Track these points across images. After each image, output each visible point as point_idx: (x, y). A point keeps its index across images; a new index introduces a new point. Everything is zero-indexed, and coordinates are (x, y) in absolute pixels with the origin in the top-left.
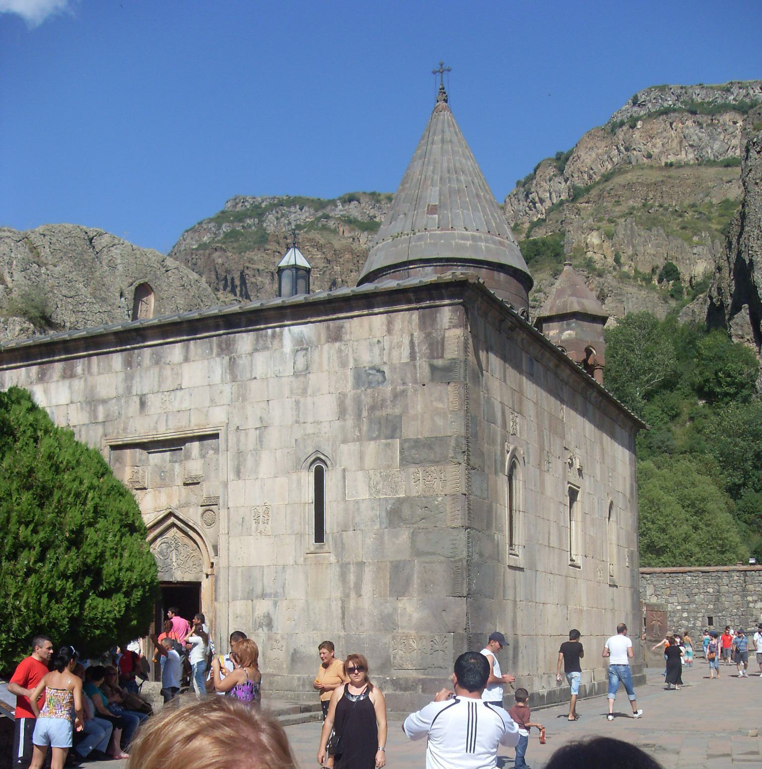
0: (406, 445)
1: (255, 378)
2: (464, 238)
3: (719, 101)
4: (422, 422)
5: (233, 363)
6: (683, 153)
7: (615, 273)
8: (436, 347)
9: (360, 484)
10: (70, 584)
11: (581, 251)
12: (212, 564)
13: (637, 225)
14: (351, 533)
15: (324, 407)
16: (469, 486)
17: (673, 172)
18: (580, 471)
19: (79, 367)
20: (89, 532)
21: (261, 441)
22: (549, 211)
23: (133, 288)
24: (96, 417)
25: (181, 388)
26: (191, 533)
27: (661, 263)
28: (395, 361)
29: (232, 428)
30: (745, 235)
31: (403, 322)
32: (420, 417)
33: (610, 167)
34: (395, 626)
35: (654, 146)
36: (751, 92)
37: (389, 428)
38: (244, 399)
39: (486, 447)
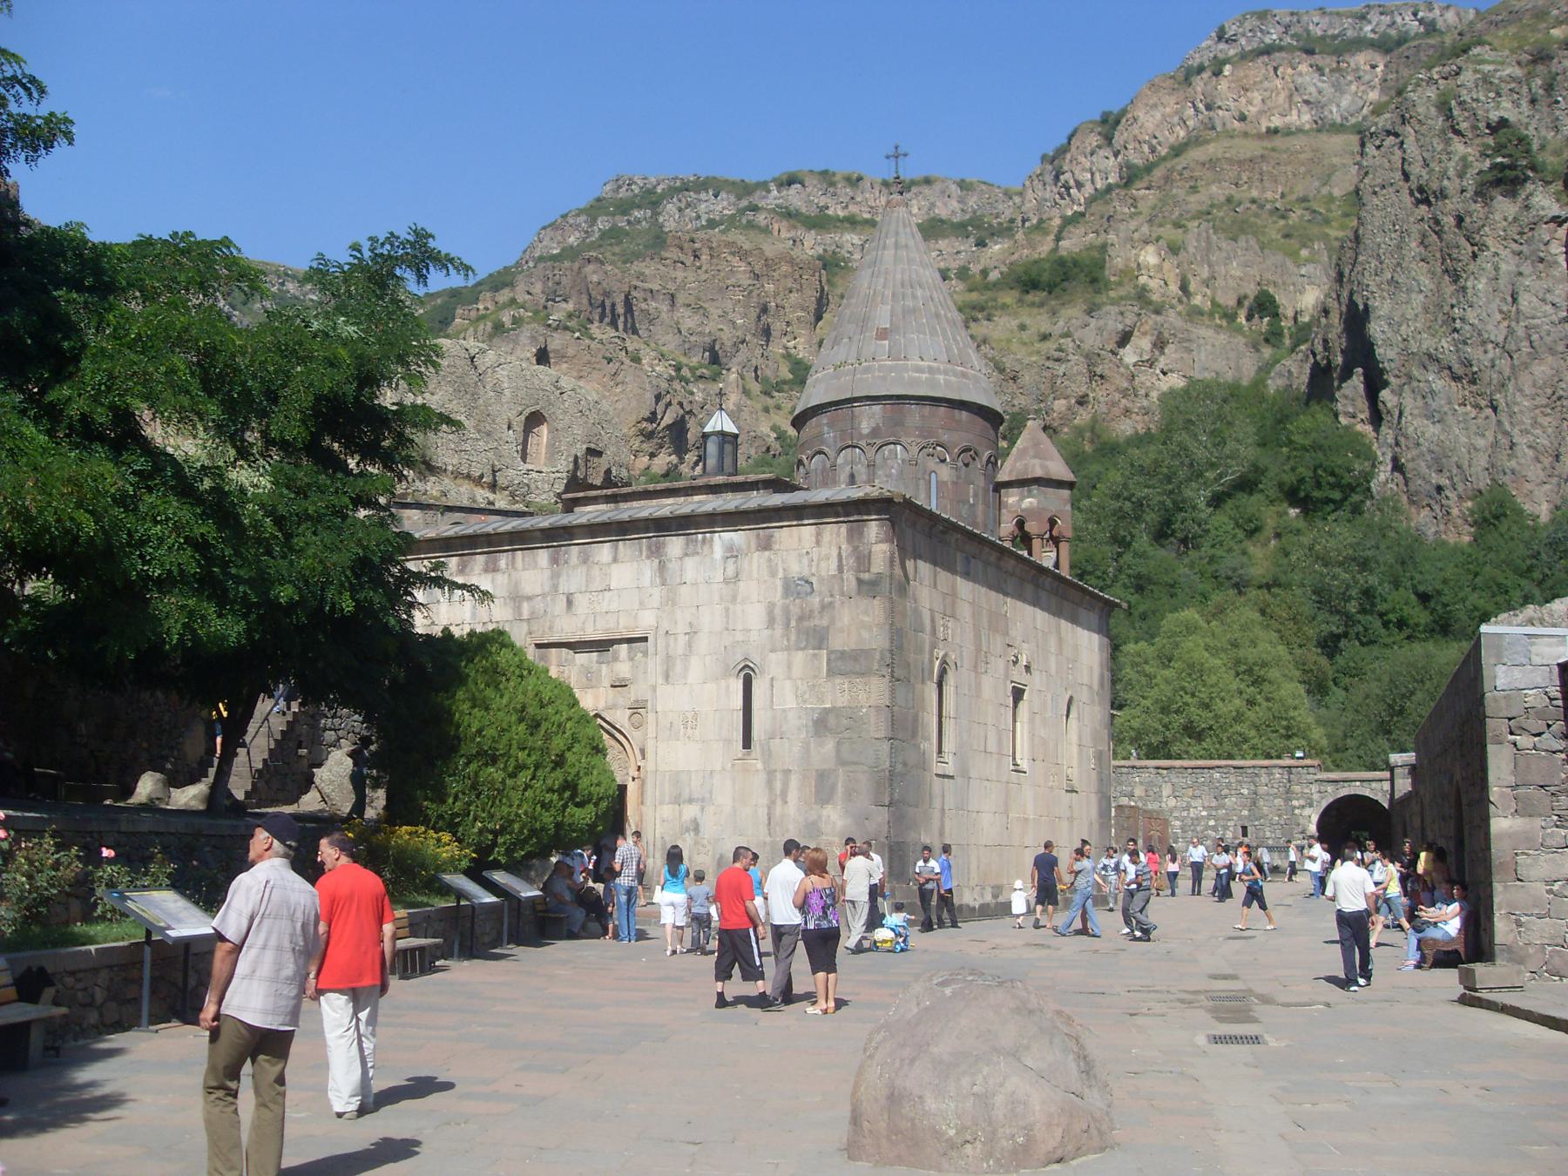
2: (919, 370)
3: (1350, 33)
5: (662, 567)
6: (1294, 112)
7: (1180, 308)
8: (863, 560)
9: (788, 693)
10: (555, 797)
11: (1131, 273)
14: (777, 740)
15: (753, 616)
17: (1278, 142)
18: (1028, 668)
20: (568, 755)
22: (1090, 201)
23: (523, 418)
24: (520, 614)
27: (1251, 290)
29: (661, 632)
30: (1359, 268)
33: (1182, 134)
35: (1250, 102)
36: (1399, 20)
37: (817, 638)
38: (674, 604)
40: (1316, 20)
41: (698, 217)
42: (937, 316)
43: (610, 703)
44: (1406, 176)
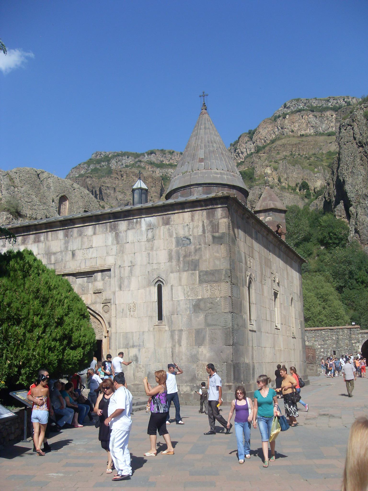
0: (201, 274)
1: (128, 242)
2: (217, 174)
3: (324, 105)
4: (209, 263)
5: (117, 235)
6: (308, 130)
7: (278, 187)
8: (215, 227)
9: (180, 292)
10: (58, 344)
12: (108, 331)
13: (288, 164)
14: (175, 316)
15: (162, 256)
16: (232, 293)
17: (304, 139)
19: (42, 237)
20: (65, 318)
21: (131, 272)
22: (246, 158)
23: (58, 198)
24: (50, 261)
25: (92, 247)
26: (97, 316)
27: (300, 182)
28: (196, 234)
29: (117, 266)
30: (340, 168)
31: (199, 216)
32: (208, 260)
33: (274, 136)
34: (198, 360)
35: (295, 126)
36: (339, 102)
37: (193, 265)
39: (239, 274)
40: (314, 102)
41: (122, 164)
42: (222, 154)
43: (93, 301)
44: (355, 138)
